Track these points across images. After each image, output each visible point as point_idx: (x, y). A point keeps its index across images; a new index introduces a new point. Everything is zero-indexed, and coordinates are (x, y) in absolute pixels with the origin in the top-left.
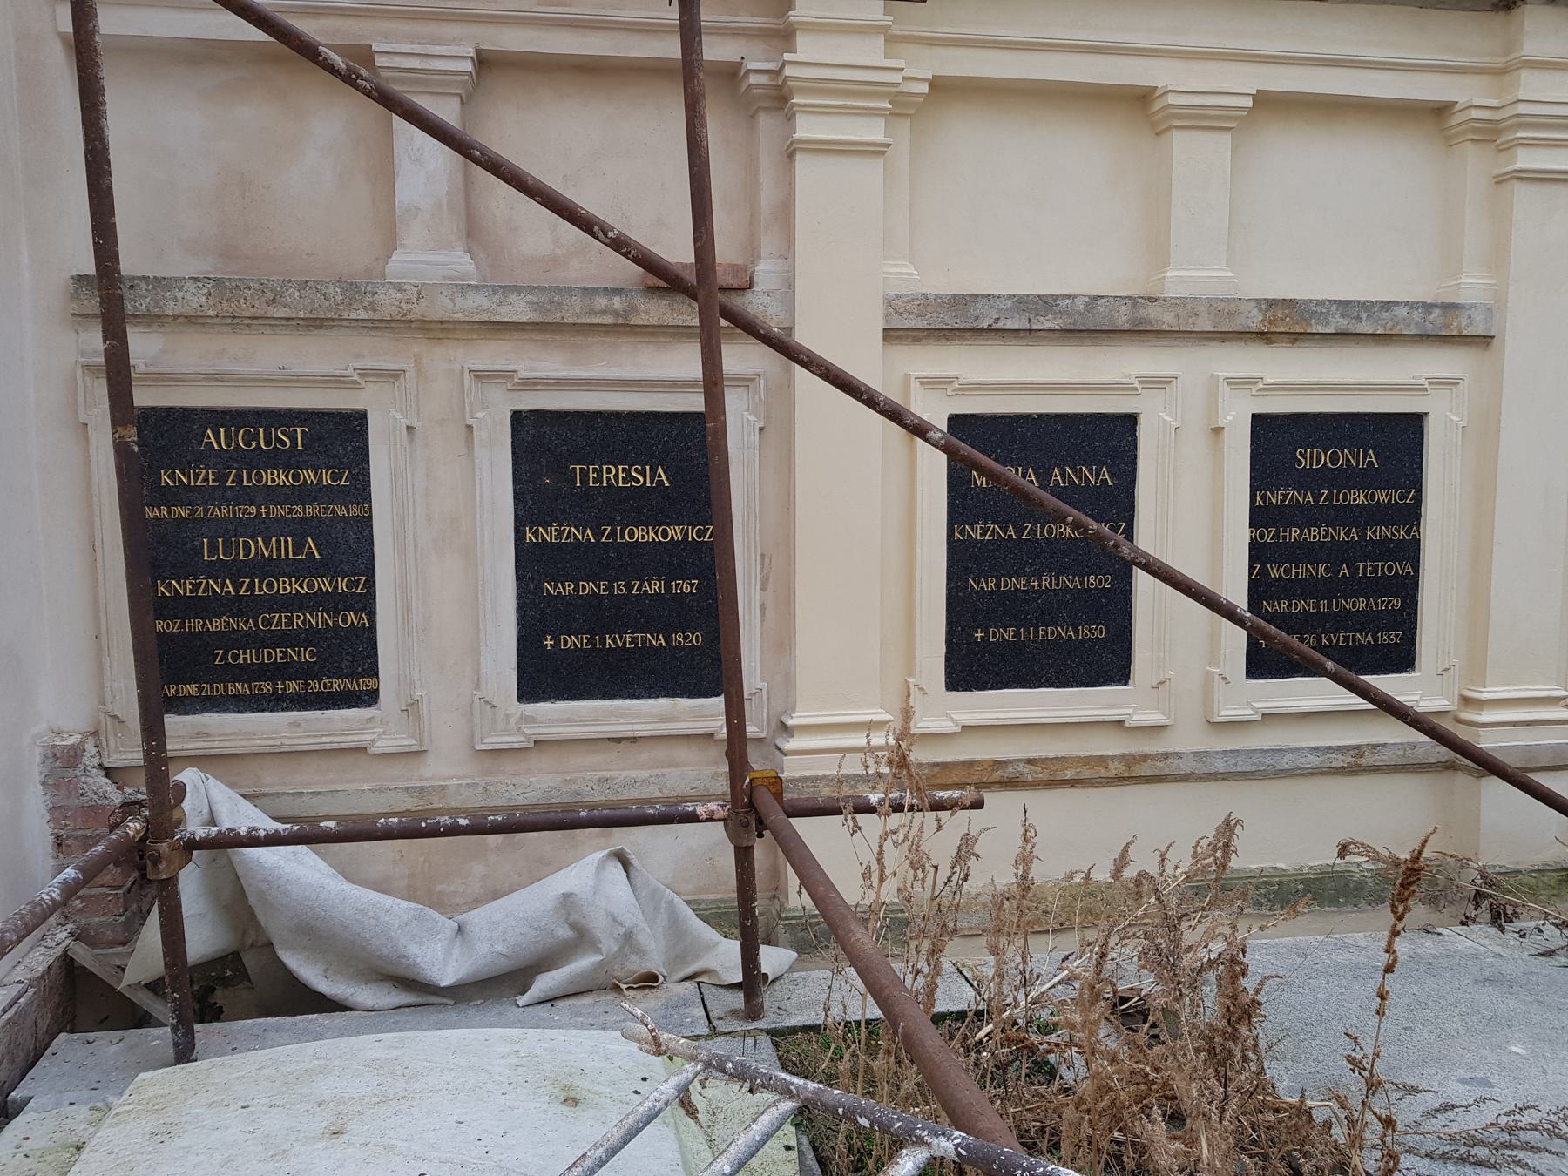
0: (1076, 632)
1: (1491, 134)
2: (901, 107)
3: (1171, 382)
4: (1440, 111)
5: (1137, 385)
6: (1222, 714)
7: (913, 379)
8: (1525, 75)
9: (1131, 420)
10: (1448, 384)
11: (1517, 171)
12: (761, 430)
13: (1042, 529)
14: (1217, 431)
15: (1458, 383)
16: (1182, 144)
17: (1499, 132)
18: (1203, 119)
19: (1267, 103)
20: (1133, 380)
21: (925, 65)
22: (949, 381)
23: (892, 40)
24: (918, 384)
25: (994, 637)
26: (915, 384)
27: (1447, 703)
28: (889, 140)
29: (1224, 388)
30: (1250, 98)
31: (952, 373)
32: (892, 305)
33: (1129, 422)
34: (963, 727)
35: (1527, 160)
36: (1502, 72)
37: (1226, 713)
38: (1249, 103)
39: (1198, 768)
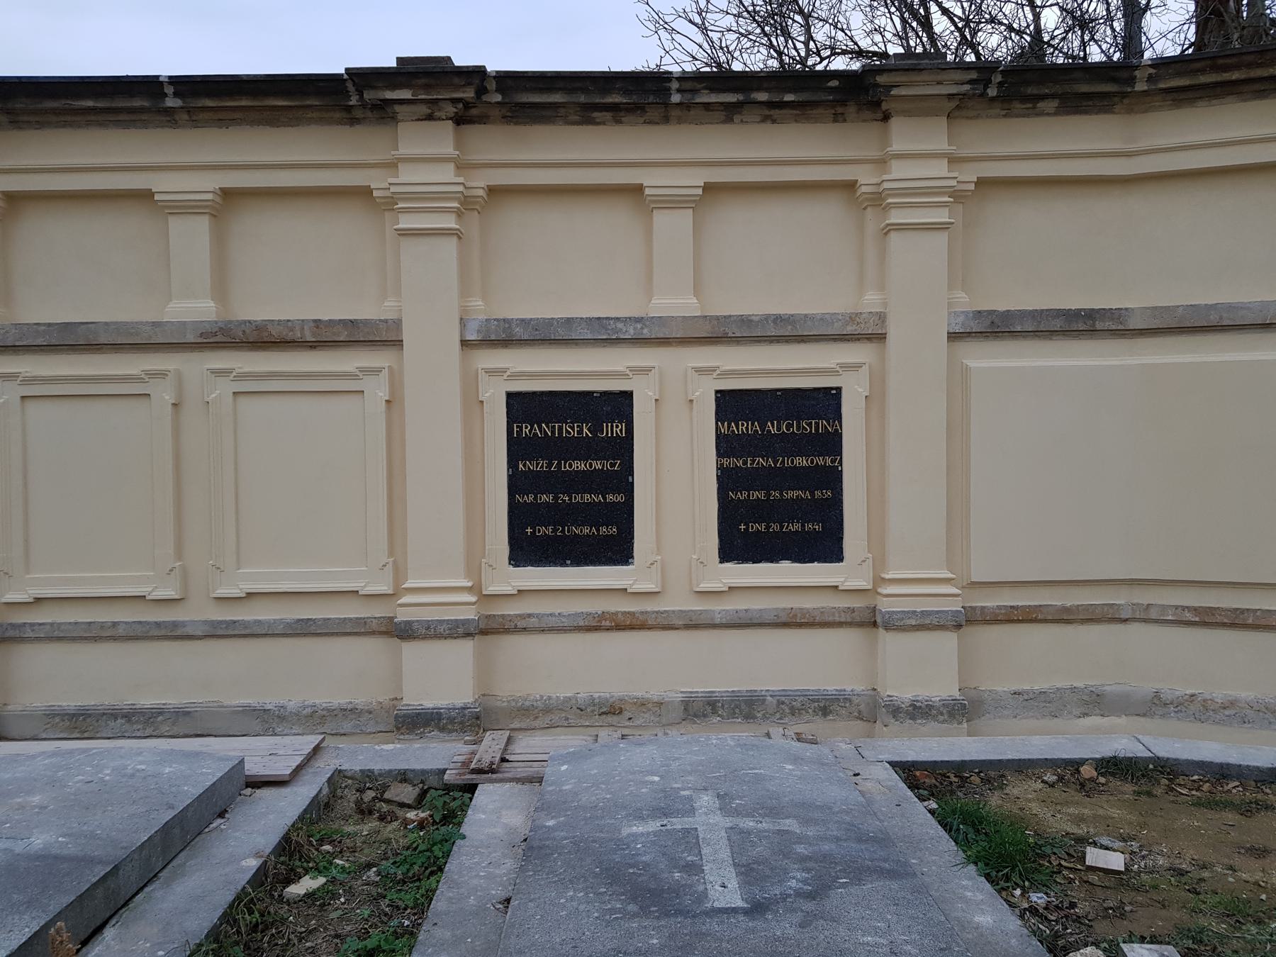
0: (598, 530)
1: (878, 200)
2: (467, 204)
3: (651, 370)
4: (851, 186)
8: (895, 164)
9: (627, 396)
10: (857, 367)
11: (888, 225)
13: (565, 465)
15: (861, 367)
16: (662, 219)
17: (884, 200)
18: (673, 203)
19: (709, 188)
21: (480, 182)
22: (504, 371)
23: (461, 167)
24: (484, 373)
25: (539, 532)
27: (865, 584)
30: (701, 189)
31: (507, 366)
33: (627, 396)
34: (518, 591)
35: (896, 217)
36: (882, 163)
37: (705, 586)
38: (700, 191)
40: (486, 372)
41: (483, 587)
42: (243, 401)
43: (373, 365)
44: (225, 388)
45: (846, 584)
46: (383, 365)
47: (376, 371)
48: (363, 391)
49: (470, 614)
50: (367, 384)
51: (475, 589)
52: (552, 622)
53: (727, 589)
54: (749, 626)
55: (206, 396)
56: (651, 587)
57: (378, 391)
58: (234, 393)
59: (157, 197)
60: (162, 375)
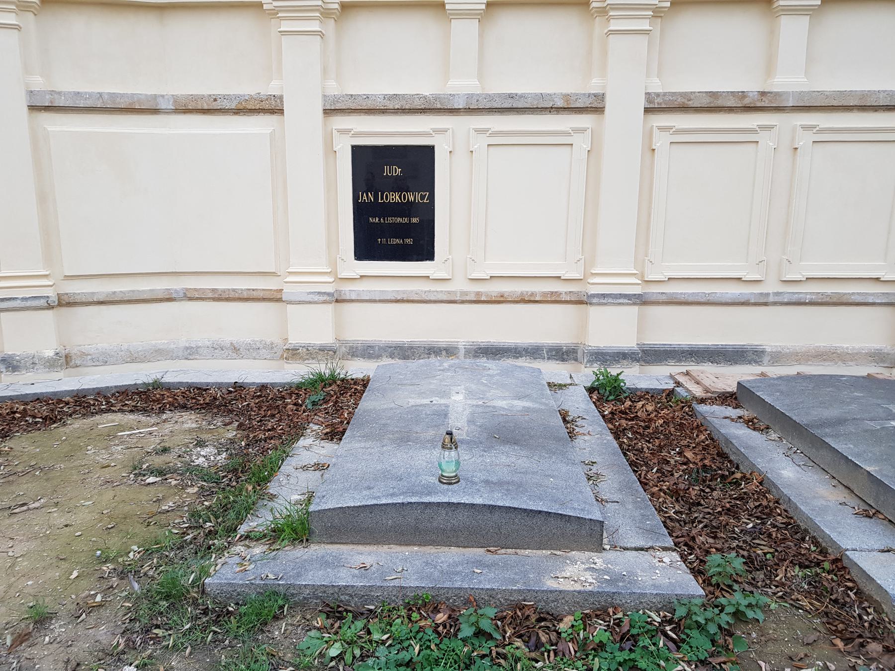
5: (757, 129)
6: (787, 277)
7: (655, 127)
12: (589, 151)
14: (654, 150)
20: (755, 127)
26: (655, 130)
28: (651, 28)
29: (800, 131)
31: (673, 125)
32: (649, 96)
39: (777, 299)
40: (658, 129)
41: (646, 276)
42: (491, 148)
43: (691, 127)
44: (485, 140)
45: (886, 277)
46: (588, 126)
47: (583, 130)
48: (572, 144)
49: (637, 290)
50: (575, 139)
51: (641, 276)
52: (682, 298)
53: (805, 279)
54: (829, 304)
55: (471, 147)
56: (757, 277)
57: (582, 143)
58: (488, 145)
59: (447, 7)
60: (445, 131)
